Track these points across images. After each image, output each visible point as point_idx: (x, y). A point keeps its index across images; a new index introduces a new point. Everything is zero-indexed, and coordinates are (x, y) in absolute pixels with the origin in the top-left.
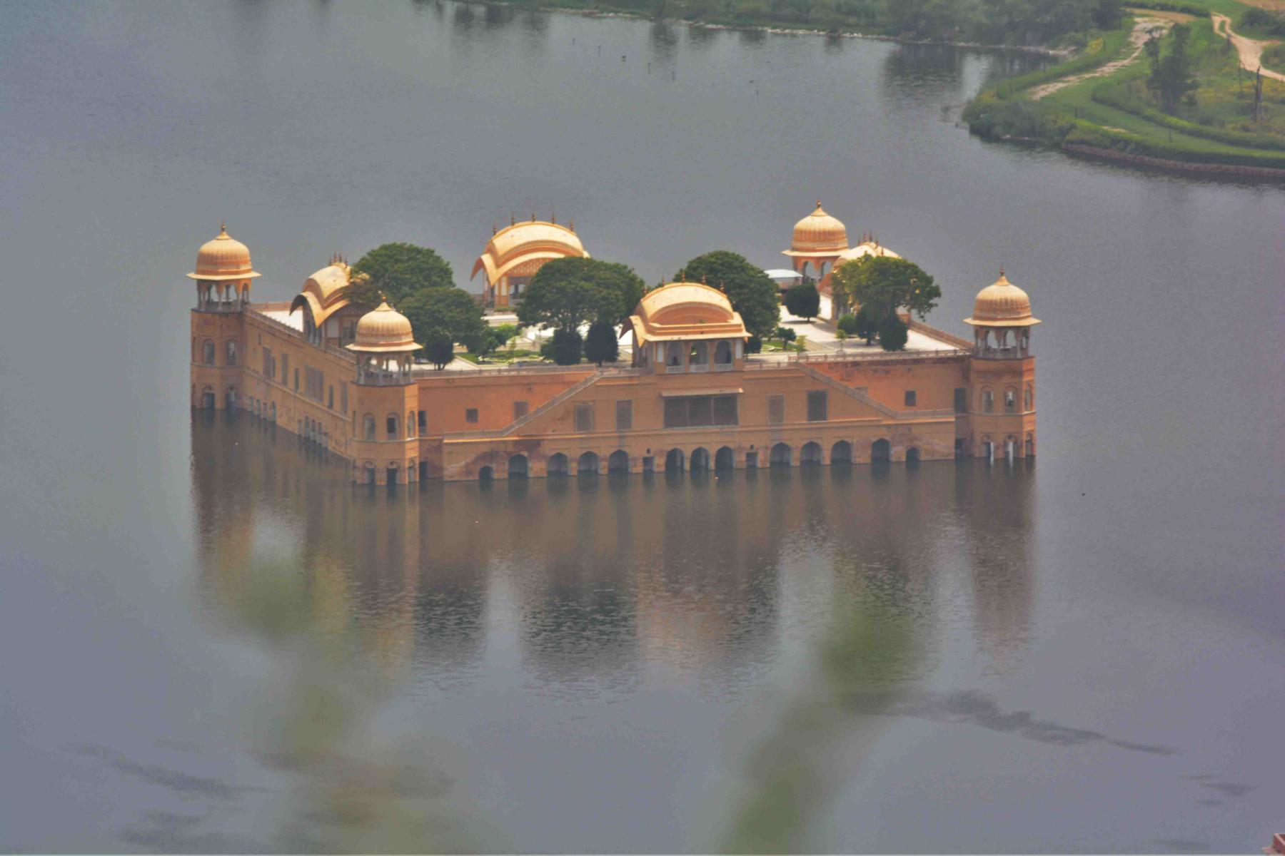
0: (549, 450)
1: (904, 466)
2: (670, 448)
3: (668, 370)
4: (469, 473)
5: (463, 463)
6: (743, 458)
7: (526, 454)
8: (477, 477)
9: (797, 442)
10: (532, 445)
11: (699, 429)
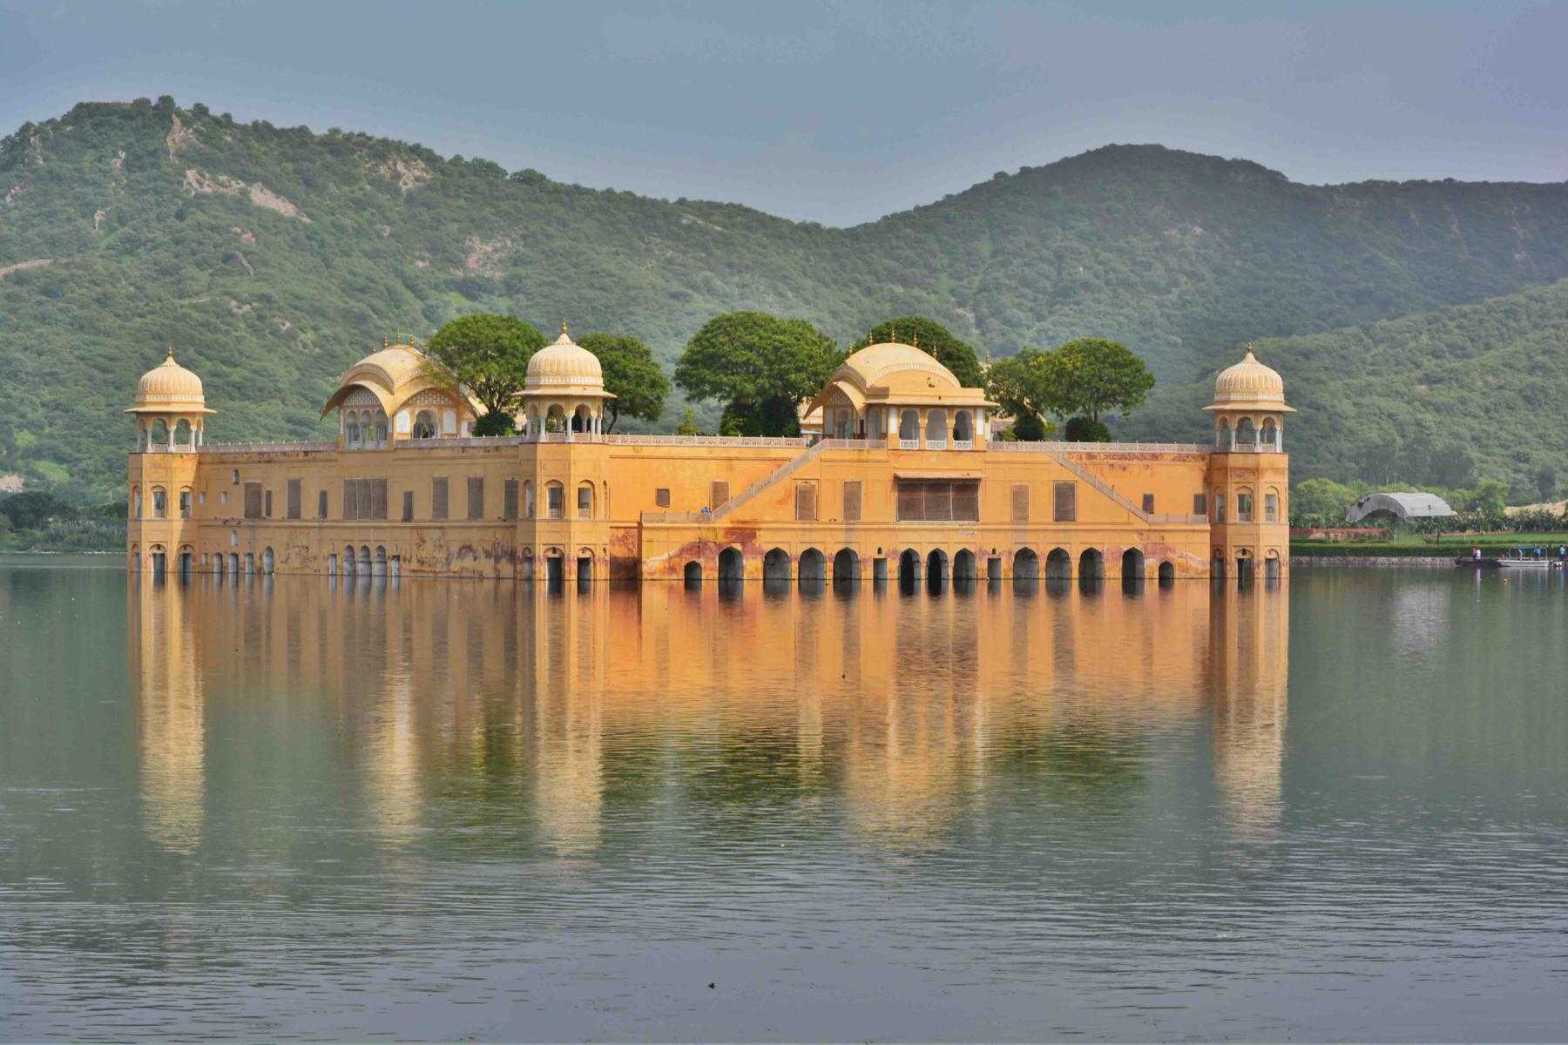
0: (766, 542)
1: (1156, 582)
2: (904, 548)
3: (901, 444)
4: (672, 569)
5: (666, 556)
6: (985, 565)
7: (738, 547)
8: (682, 576)
9: (1042, 549)
10: (746, 533)
11: (937, 524)
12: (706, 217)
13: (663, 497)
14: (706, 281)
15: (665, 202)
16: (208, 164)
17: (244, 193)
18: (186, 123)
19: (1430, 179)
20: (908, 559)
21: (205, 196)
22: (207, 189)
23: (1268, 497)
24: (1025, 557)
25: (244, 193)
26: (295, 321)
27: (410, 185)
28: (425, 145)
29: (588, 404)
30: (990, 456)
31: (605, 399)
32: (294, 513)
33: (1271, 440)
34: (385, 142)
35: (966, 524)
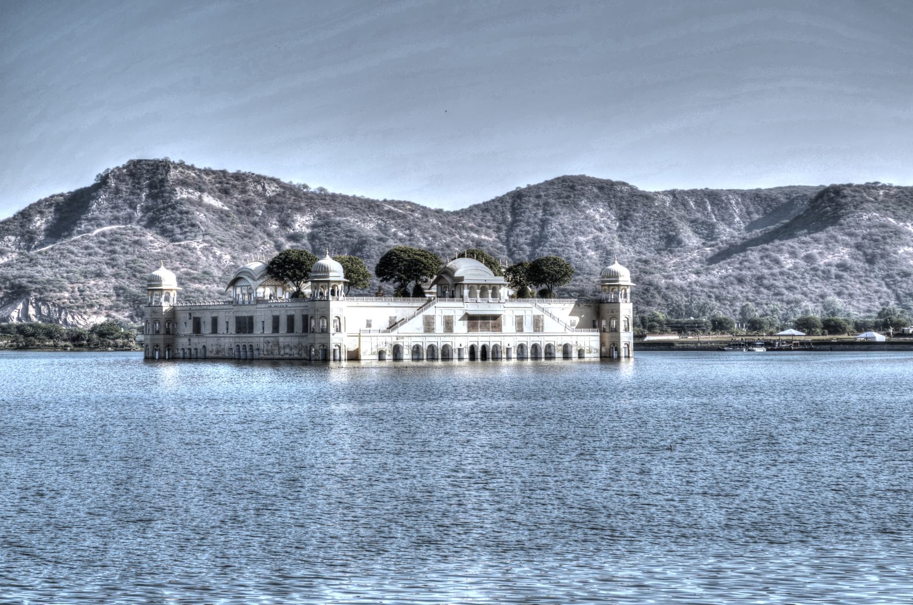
3: (469, 300)
11: (485, 333)
12: (395, 206)
13: (369, 325)
14: (395, 234)
15: (378, 201)
16: (184, 183)
17: (200, 197)
18: (176, 168)
19: (699, 188)
20: (472, 350)
21: (182, 199)
22: (185, 196)
25: (200, 197)
26: (222, 250)
27: (272, 194)
28: (276, 177)
30: (506, 305)
31: (345, 283)
32: (215, 330)
33: (625, 296)
34: (258, 176)
35: (498, 334)
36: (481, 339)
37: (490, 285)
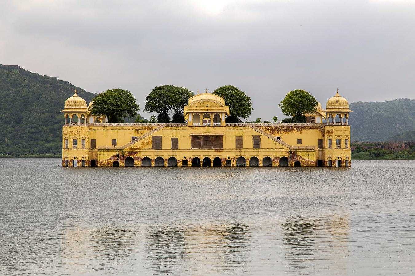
0: (142, 155)
13: (114, 142)
23: (346, 140)
24: (241, 160)
29: (77, 114)
30: (227, 128)
36: (202, 153)
37: (212, 113)
